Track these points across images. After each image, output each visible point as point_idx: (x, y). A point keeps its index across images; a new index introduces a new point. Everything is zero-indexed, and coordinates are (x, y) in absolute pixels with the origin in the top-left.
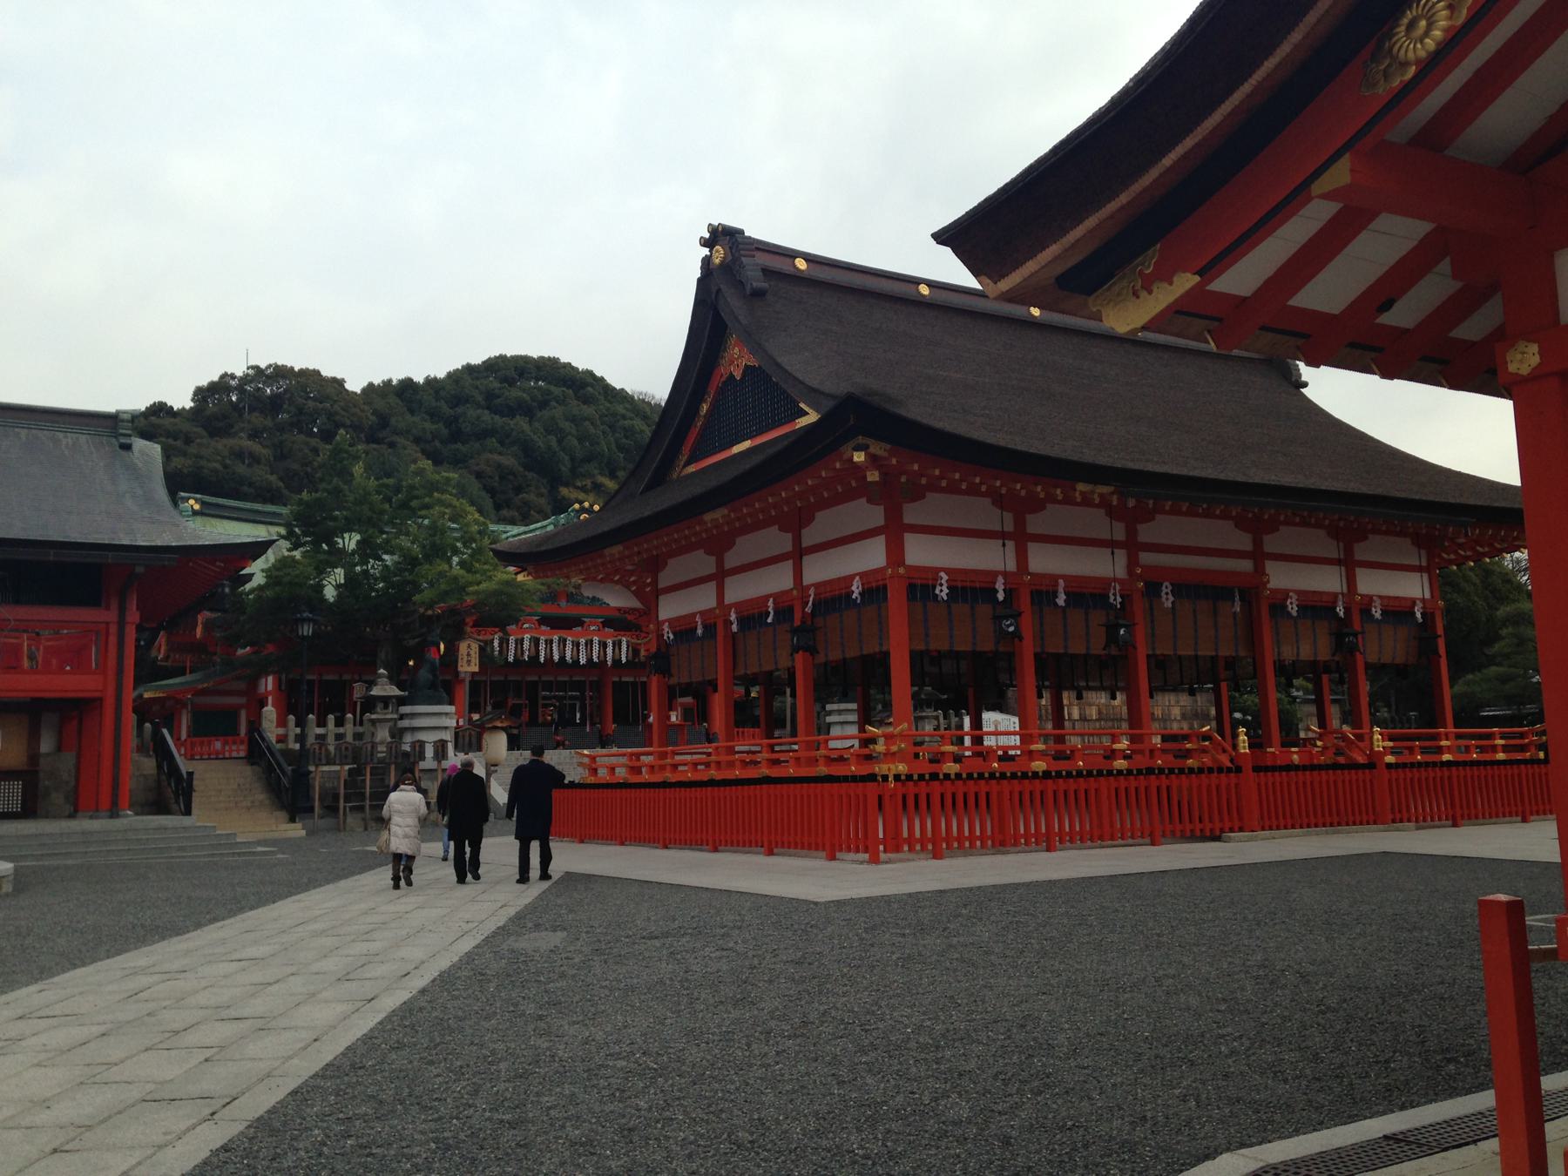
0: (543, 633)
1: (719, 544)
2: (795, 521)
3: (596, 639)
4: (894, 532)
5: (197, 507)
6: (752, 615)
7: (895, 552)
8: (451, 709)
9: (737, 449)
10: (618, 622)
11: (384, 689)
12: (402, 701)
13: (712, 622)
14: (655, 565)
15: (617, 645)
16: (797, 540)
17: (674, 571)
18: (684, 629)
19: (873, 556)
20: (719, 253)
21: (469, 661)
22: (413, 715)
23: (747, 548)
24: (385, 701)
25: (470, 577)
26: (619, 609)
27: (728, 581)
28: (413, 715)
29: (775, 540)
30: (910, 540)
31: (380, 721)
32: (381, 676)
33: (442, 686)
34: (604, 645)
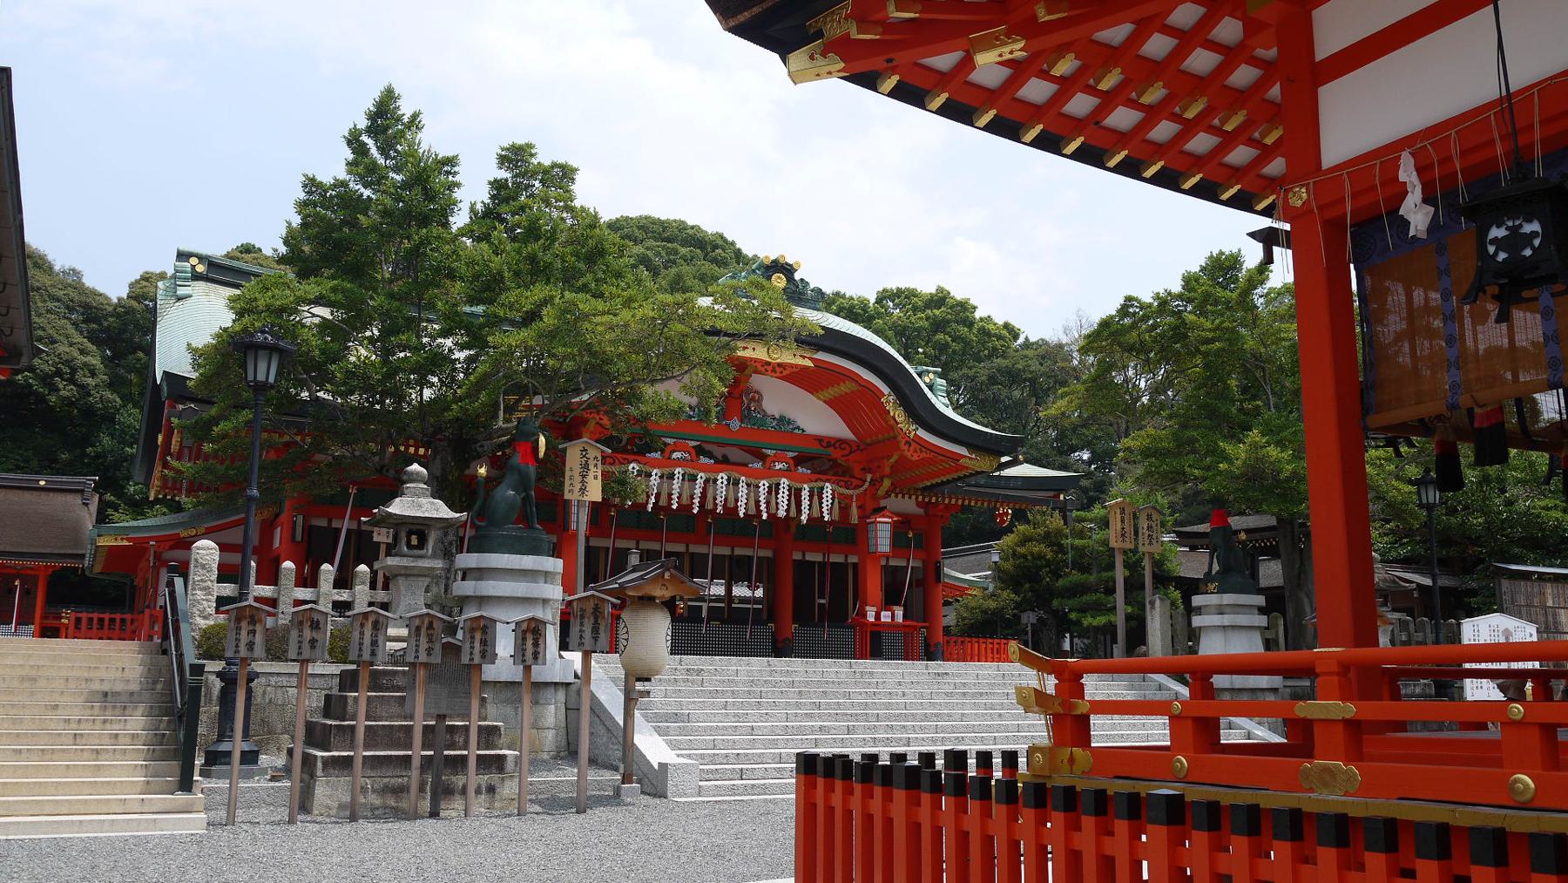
0: (704, 469)
3: (784, 482)
5: (200, 268)
8: (556, 565)
10: (817, 459)
11: (417, 503)
12: (454, 540)
15: (816, 494)
21: (586, 486)
22: (481, 573)
24: (417, 530)
25: (600, 305)
26: (819, 440)
28: (481, 573)
31: (408, 573)
32: (415, 478)
33: (542, 520)
34: (796, 495)
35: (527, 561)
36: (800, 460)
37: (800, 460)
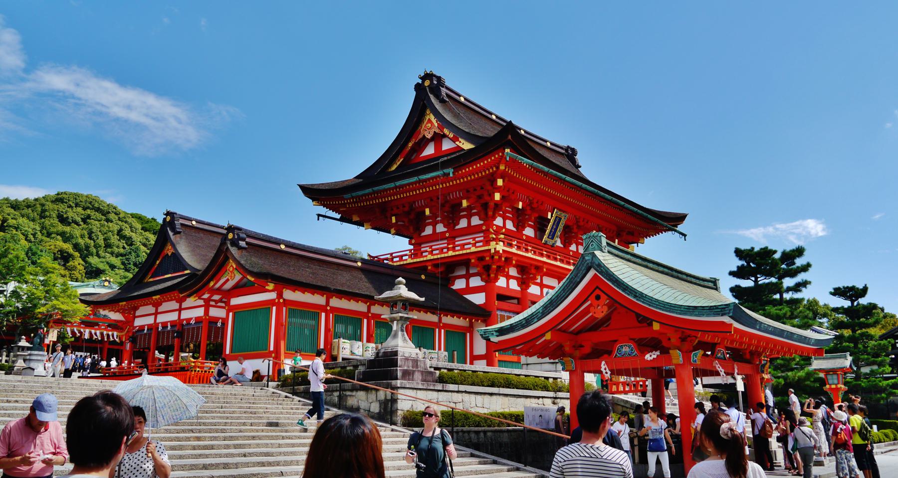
1: (157, 305)
2: (180, 301)
4: (207, 306)
6: (164, 325)
7: (207, 312)
9: (166, 276)
10: (115, 326)
11: (23, 343)
12: (29, 349)
13: (153, 327)
14: (136, 308)
16: (180, 306)
17: (142, 311)
18: (142, 328)
19: (200, 312)
20: (168, 218)
23: (165, 306)
26: (115, 321)
27: (159, 316)
29: (174, 305)
30: (211, 308)
35: (41, 353)
36: (109, 326)
37: (109, 326)
